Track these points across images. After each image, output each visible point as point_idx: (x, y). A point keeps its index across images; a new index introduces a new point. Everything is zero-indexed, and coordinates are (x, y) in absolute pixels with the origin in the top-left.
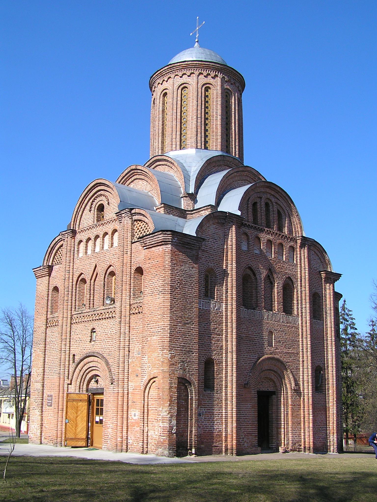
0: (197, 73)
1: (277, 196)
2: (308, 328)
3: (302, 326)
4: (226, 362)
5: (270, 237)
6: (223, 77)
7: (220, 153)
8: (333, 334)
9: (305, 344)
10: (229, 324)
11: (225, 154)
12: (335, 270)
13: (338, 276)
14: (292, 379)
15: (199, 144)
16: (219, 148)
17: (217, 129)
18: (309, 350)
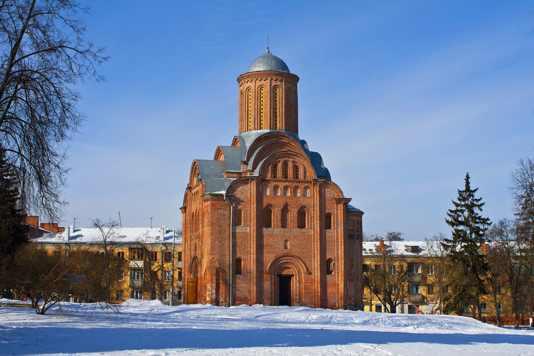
0: (255, 79)
1: (295, 157)
2: (318, 236)
3: (314, 235)
4: (250, 259)
5: (287, 184)
6: (272, 79)
7: (268, 131)
8: (342, 238)
9: (317, 245)
10: (252, 239)
11: (272, 131)
12: (346, 196)
13: (350, 200)
14: (305, 267)
15: (256, 127)
16: (269, 127)
17: (267, 115)
18: (319, 249)
